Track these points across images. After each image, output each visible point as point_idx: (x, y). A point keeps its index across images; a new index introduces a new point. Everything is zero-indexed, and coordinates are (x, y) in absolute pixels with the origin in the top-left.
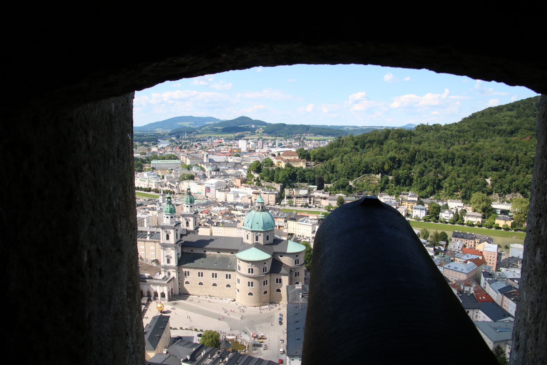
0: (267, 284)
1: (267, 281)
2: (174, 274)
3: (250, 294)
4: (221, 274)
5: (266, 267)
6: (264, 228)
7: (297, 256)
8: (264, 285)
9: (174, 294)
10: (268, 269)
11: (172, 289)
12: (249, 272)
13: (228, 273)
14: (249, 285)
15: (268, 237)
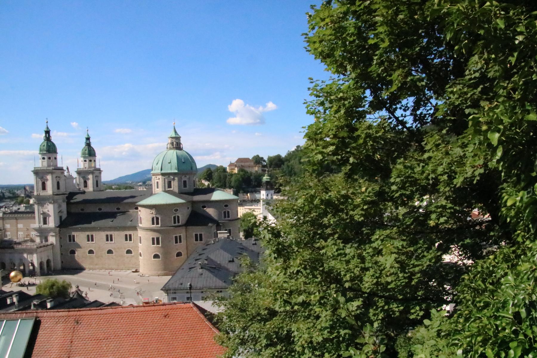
0: (180, 241)
1: (180, 237)
2: (52, 240)
3: (156, 256)
4: (119, 236)
5: (178, 217)
6: (178, 169)
7: (226, 206)
8: (176, 242)
9: (52, 269)
10: (183, 219)
11: (48, 262)
12: (153, 224)
13: (128, 233)
14: (153, 244)
15: (185, 182)
